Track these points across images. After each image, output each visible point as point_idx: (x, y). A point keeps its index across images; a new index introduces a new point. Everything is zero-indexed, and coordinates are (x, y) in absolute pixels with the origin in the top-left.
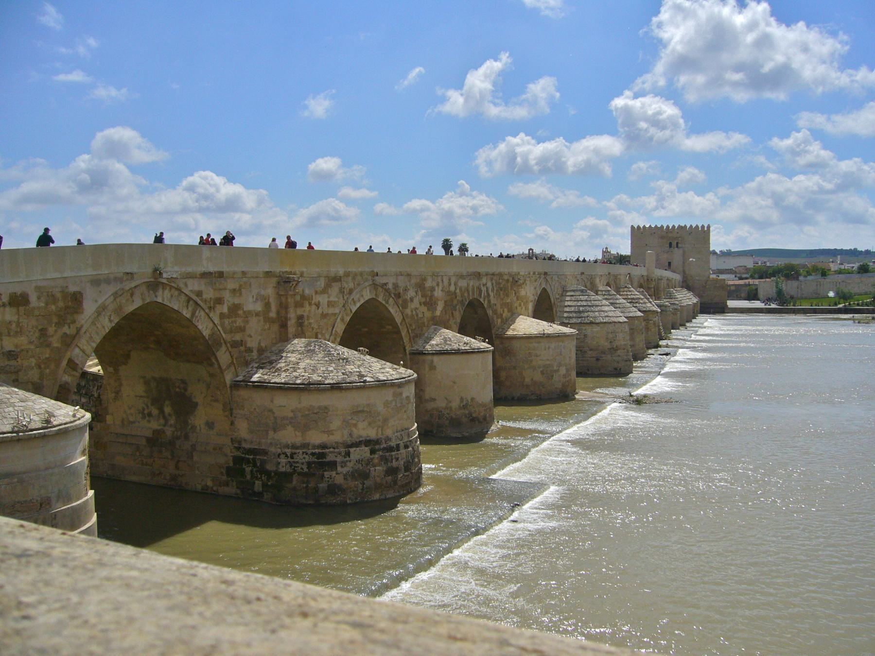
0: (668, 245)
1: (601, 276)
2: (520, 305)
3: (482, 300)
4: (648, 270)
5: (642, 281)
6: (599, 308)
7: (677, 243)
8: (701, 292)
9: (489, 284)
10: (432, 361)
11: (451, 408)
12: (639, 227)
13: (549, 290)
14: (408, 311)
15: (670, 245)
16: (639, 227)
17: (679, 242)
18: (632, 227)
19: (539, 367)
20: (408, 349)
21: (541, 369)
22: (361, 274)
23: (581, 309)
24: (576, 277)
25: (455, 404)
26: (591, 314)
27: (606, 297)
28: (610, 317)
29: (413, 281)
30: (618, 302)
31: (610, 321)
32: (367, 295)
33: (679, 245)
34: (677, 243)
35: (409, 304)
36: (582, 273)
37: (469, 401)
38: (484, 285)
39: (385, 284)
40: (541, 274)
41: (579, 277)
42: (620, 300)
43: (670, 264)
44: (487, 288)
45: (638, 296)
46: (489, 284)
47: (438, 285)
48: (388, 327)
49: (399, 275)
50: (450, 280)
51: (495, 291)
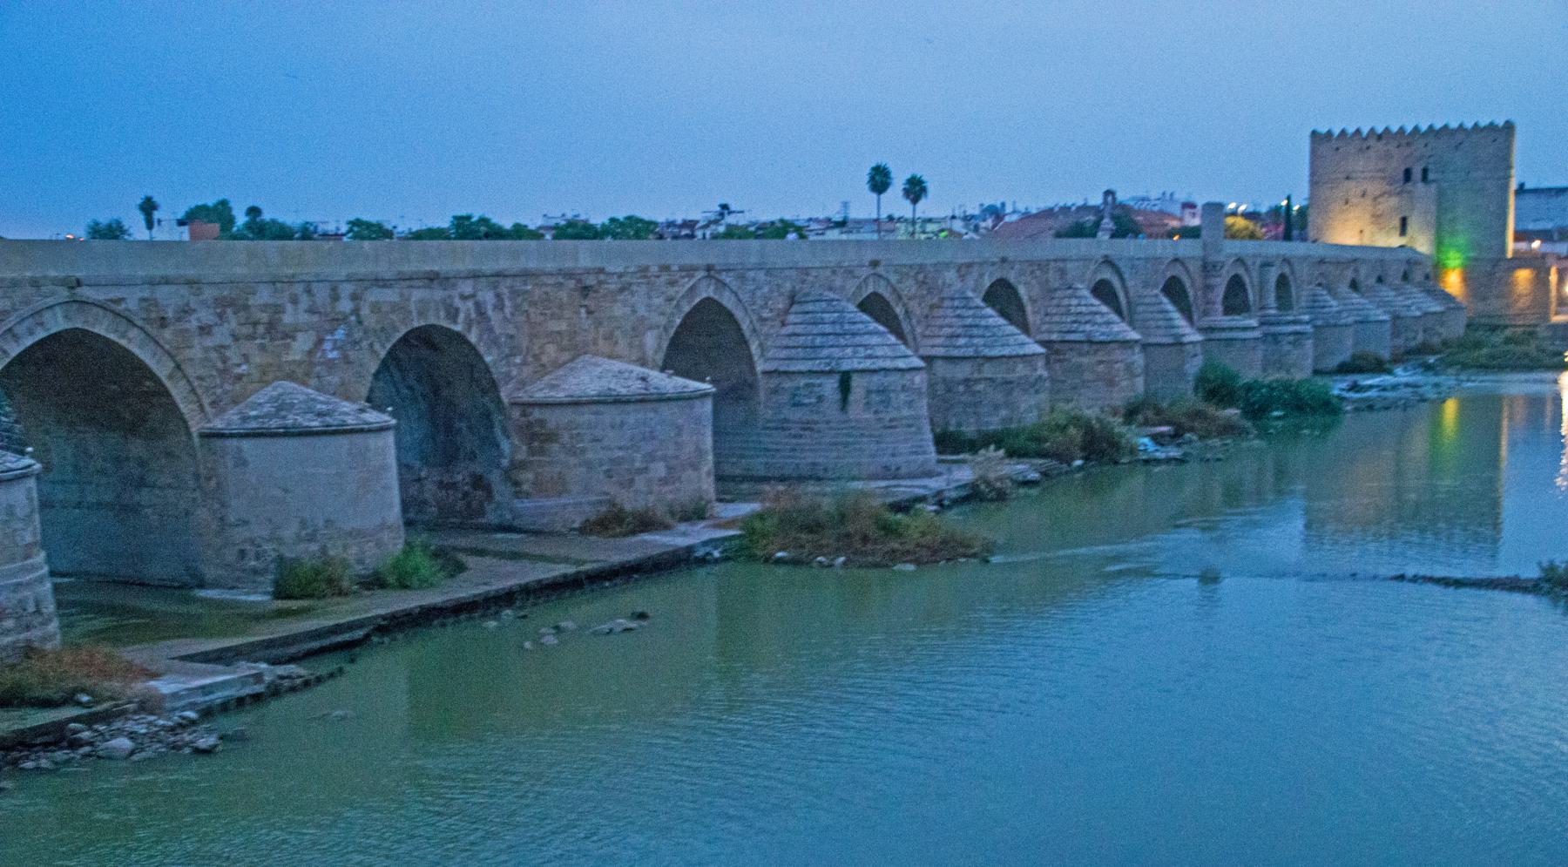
0: (1401, 175)
1: (969, 265)
2: (609, 337)
3: (458, 328)
4: (1205, 246)
5: (1177, 271)
6: (858, 340)
7: (1425, 171)
9: (488, 297)
10: (239, 450)
11: (280, 540)
14: (196, 352)
15: (1408, 175)
17: (1430, 167)
18: (1314, 133)
19: (601, 465)
20: (195, 427)
21: (605, 468)
22: (35, 283)
23: (818, 341)
25: (288, 533)
26: (836, 352)
27: (958, 312)
28: (877, 357)
29: (209, 293)
30: (983, 323)
31: (873, 367)
32: (58, 323)
33: (1431, 176)
34: (1425, 171)
35: (196, 341)
36: (875, 264)
37: (321, 524)
38: (464, 298)
39: (119, 301)
41: (864, 272)
42: (991, 320)
44: (478, 305)
45: (1094, 309)
46: (488, 297)
47: (295, 301)
48: (148, 383)
49: (159, 283)
50: (334, 289)
51: (507, 311)
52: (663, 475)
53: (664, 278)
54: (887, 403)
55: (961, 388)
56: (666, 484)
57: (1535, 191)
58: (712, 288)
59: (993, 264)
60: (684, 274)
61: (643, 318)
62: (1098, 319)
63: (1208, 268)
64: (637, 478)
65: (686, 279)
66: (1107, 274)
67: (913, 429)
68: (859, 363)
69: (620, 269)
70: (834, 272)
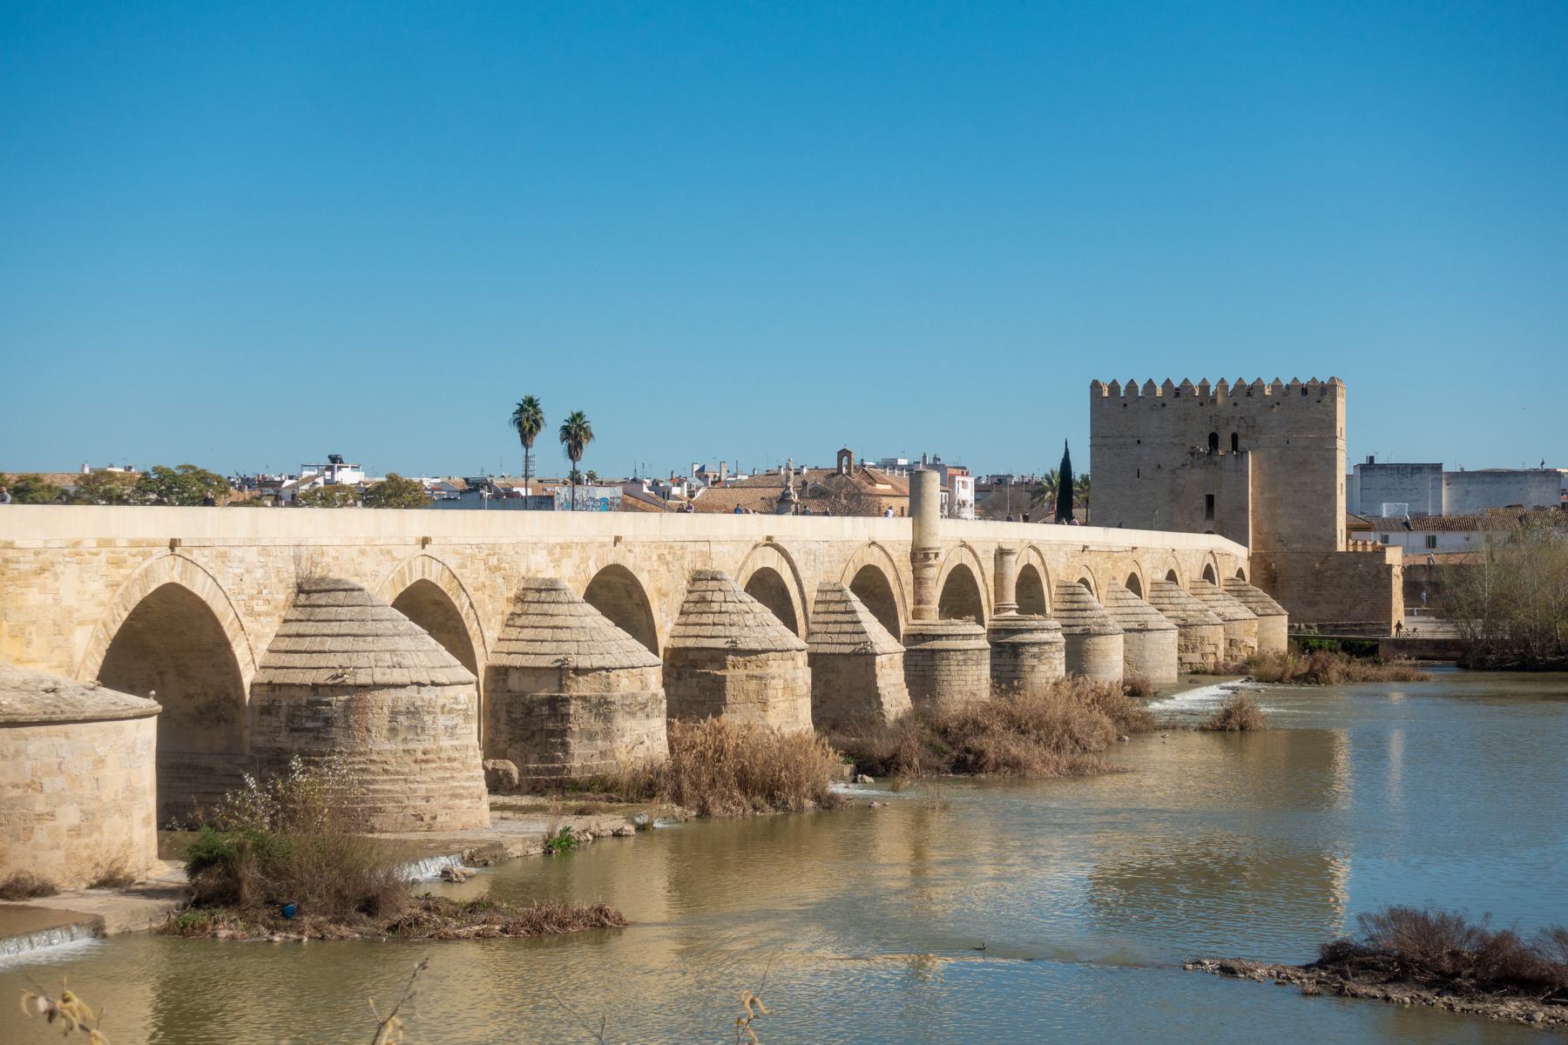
1: (565, 547)
5: (875, 558)
6: (382, 643)
7: (1235, 437)
8: (1311, 591)
12: (1114, 386)
13: (201, 588)
15: (1214, 440)
16: (1114, 386)
24: (389, 552)
33: (1242, 443)
34: (1235, 437)
36: (425, 541)
40: (153, 544)
42: (588, 620)
43: (1210, 500)
45: (743, 607)
52: (76, 822)
53: (105, 554)
54: (417, 729)
55: (545, 710)
56: (79, 835)
57: (1382, 467)
58: (178, 569)
59: (603, 545)
60: (134, 550)
61: (69, 612)
62: (749, 619)
63: (920, 556)
64: (37, 826)
65: (140, 559)
66: (772, 560)
67: (455, 764)
68: (384, 674)
69: (39, 544)
70: (363, 553)
